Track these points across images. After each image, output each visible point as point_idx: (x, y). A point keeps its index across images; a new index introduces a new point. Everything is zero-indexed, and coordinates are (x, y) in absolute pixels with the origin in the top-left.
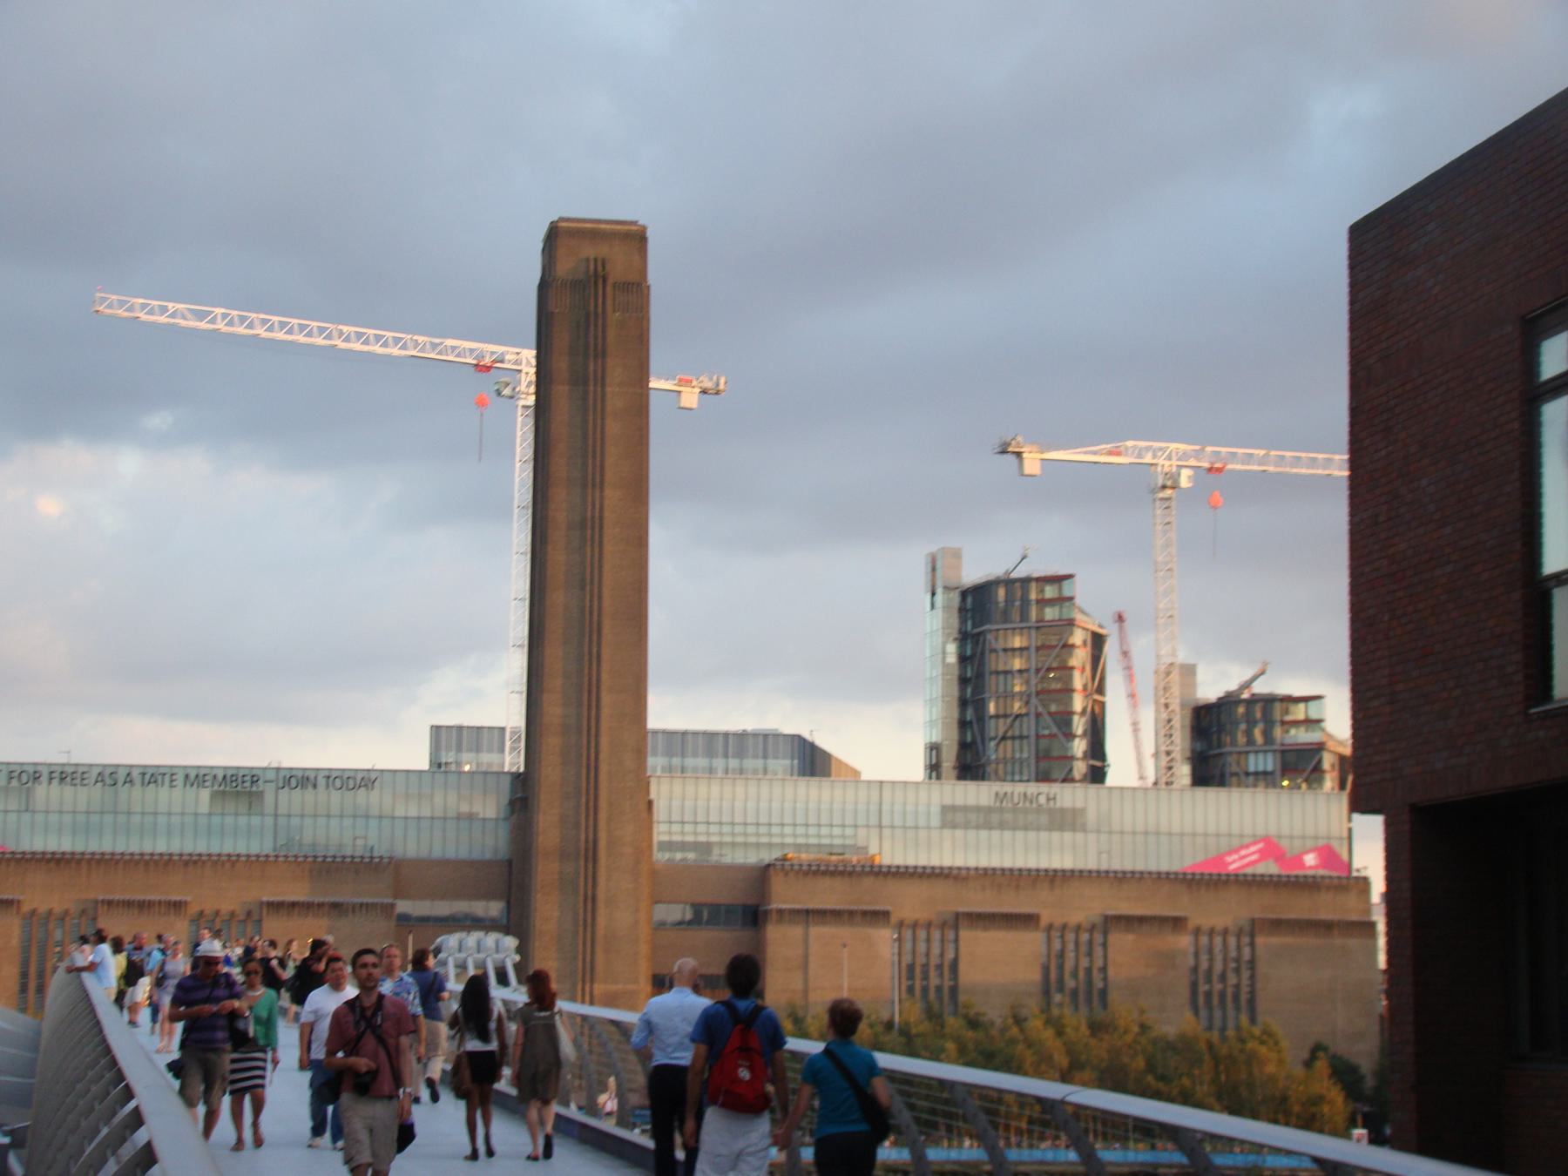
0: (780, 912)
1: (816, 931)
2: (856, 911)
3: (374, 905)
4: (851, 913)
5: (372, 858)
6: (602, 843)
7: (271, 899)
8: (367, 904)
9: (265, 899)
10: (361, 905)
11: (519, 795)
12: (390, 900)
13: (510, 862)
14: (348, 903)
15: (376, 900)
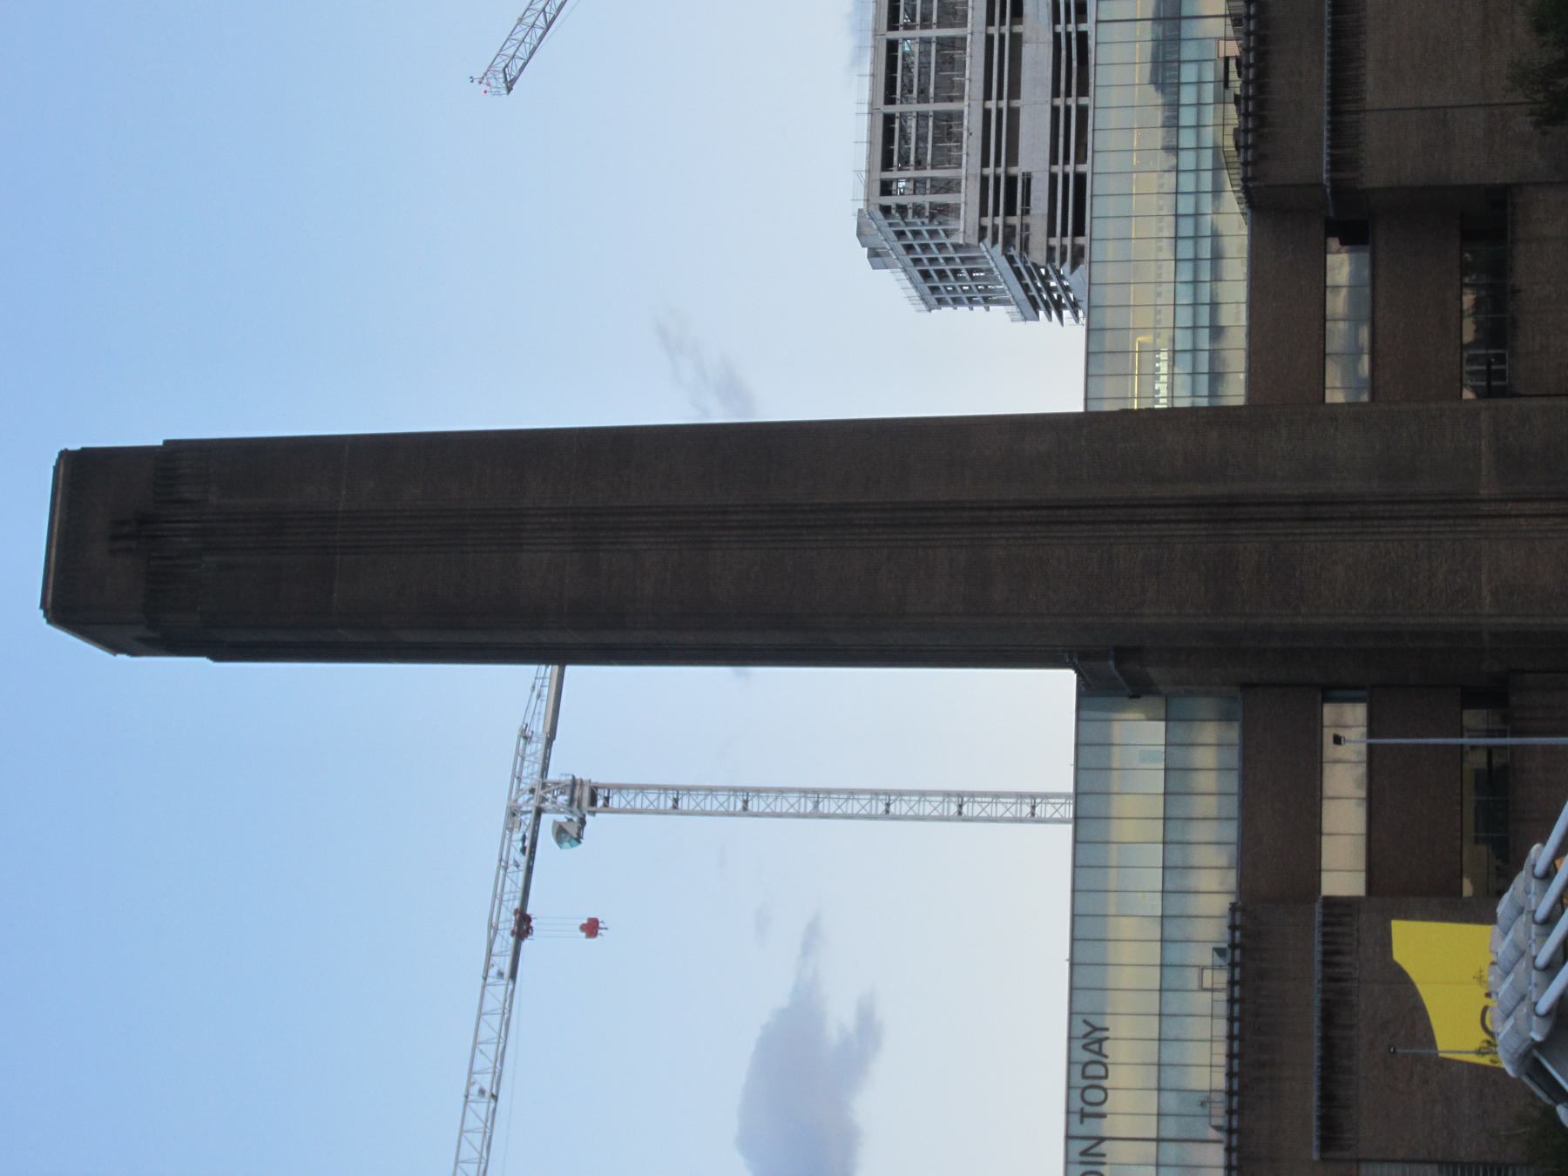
0: (1335, 164)
1: (1374, 91)
2: (1333, 22)
3: (1327, 939)
4: (1337, 33)
5: (1233, 946)
6: (1201, 490)
7: (1315, 1142)
8: (1325, 953)
9: (1316, 1156)
10: (1325, 964)
11: (1111, 663)
12: (1318, 908)
13: (1246, 686)
14: (1324, 991)
15: (1318, 937)
